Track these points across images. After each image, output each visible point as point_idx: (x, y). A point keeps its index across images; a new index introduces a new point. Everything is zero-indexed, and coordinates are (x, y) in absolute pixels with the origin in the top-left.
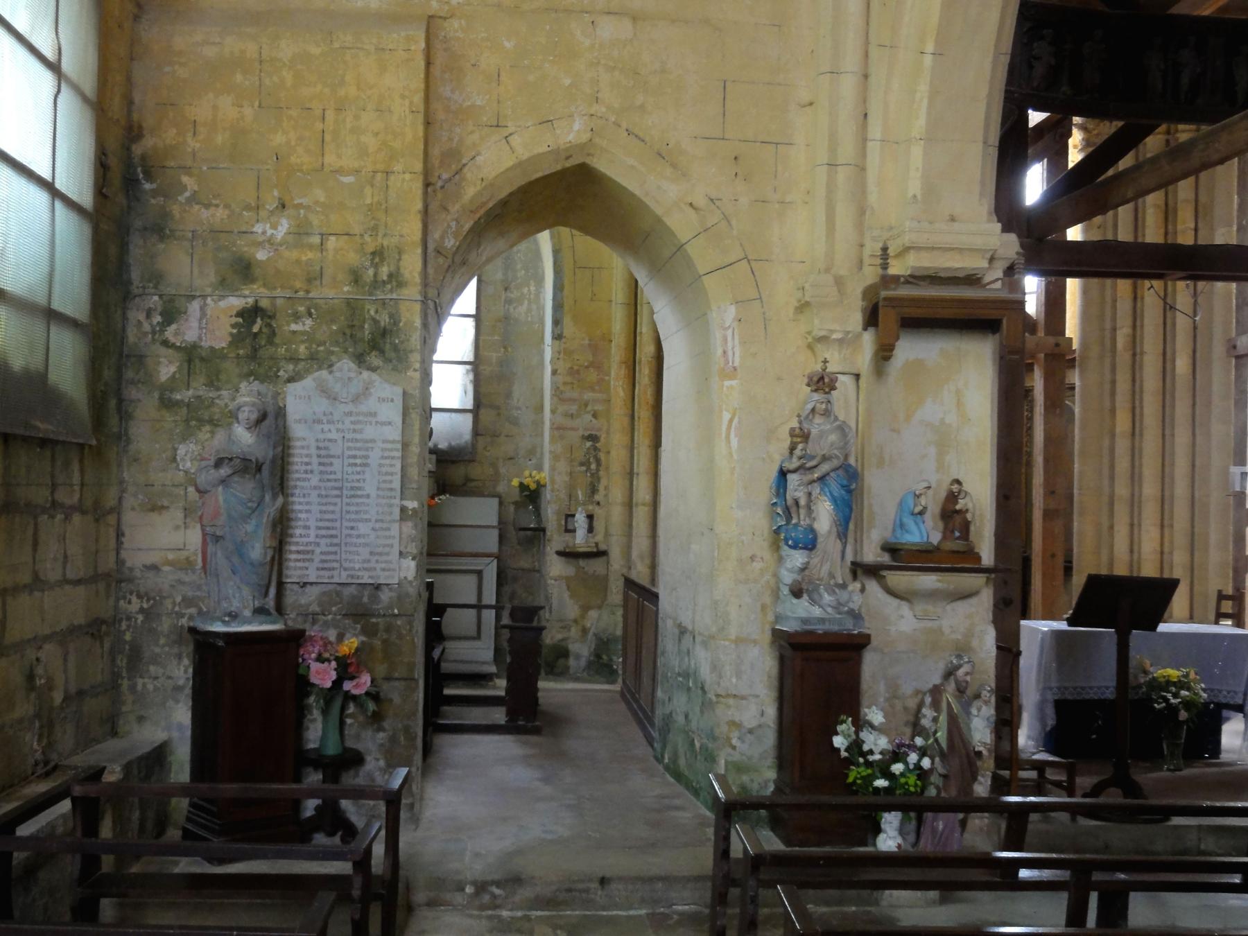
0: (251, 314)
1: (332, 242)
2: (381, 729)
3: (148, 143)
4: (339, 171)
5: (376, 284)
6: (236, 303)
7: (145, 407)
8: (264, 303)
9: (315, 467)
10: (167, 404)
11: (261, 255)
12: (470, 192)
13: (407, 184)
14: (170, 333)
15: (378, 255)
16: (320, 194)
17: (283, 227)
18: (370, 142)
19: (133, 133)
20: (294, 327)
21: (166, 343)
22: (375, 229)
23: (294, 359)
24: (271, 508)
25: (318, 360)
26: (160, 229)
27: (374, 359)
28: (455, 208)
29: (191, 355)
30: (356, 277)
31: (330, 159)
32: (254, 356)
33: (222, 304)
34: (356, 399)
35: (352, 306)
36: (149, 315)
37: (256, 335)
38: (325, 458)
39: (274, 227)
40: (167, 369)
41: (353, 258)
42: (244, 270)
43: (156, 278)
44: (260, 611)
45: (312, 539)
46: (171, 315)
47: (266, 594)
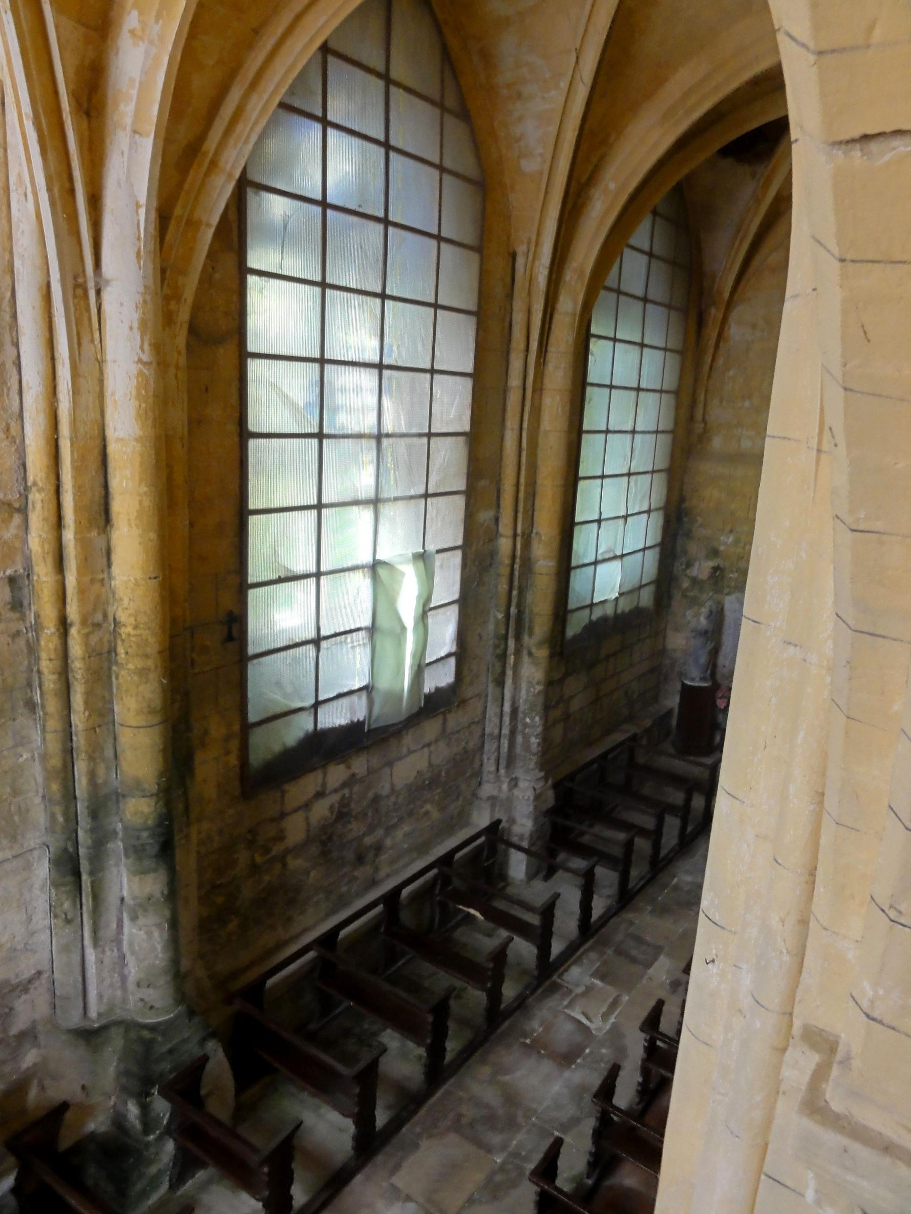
0: (716, 569)
3: (686, 505)
6: (711, 564)
7: (677, 596)
8: (721, 566)
10: (684, 596)
11: (722, 548)
14: (688, 571)
17: (731, 539)
19: (682, 500)
21: (686, 575)
23: (729, 586)
24: (710, 646)
26: (688, 535)
29: (695, 581)
32: (716, 583)
33: (706, 564)
36: (681, 565)
37: (717, 577)
39: (728, 538)
40: (686, 584)
42: (715, 553)
43: (685, 552)
44: (703, 679)
46: (689, 565)
47: (706, 671)
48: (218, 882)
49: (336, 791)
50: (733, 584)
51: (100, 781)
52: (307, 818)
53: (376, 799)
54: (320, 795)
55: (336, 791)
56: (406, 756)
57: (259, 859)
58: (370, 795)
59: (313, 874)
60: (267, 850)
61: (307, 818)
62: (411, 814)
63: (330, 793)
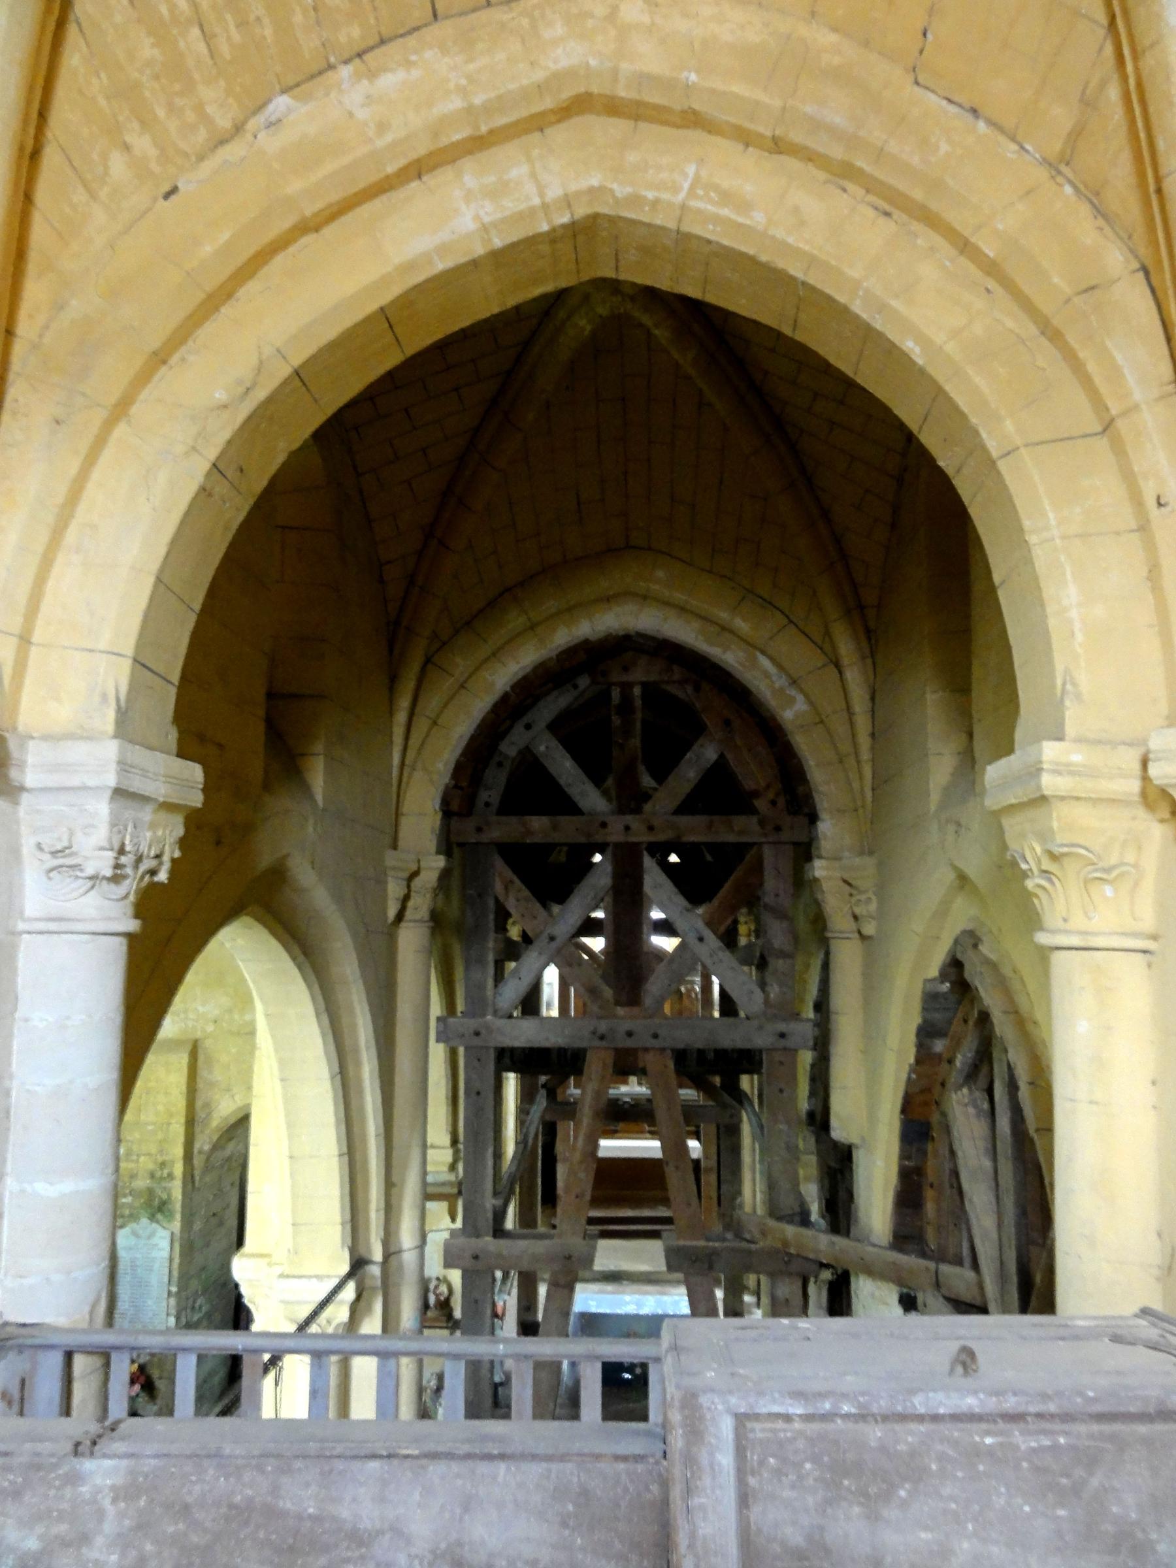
1: (142, 1159)
2: (155, 1404)
4: (147, 1124)
5: (162, 1179)
9: (129, 1271)
12: (215, 1123)
13: (178, 1129)
15: (163, 1165)
16: (137, 1135)
18: (160, 1108)
20: (124, 1200)
22: (162, 1151)
23: (122, 1216)
25: (134, 1217)
27: (159, 1216)
28: (207, 1132)
30: (152, 1176)
31: (143, 1117)
34: (149, 1237)
35: (150, 1192)
38: (134, 1267)
41: (151, 1166)
45: (127, 1307)
50: (127, 1212)
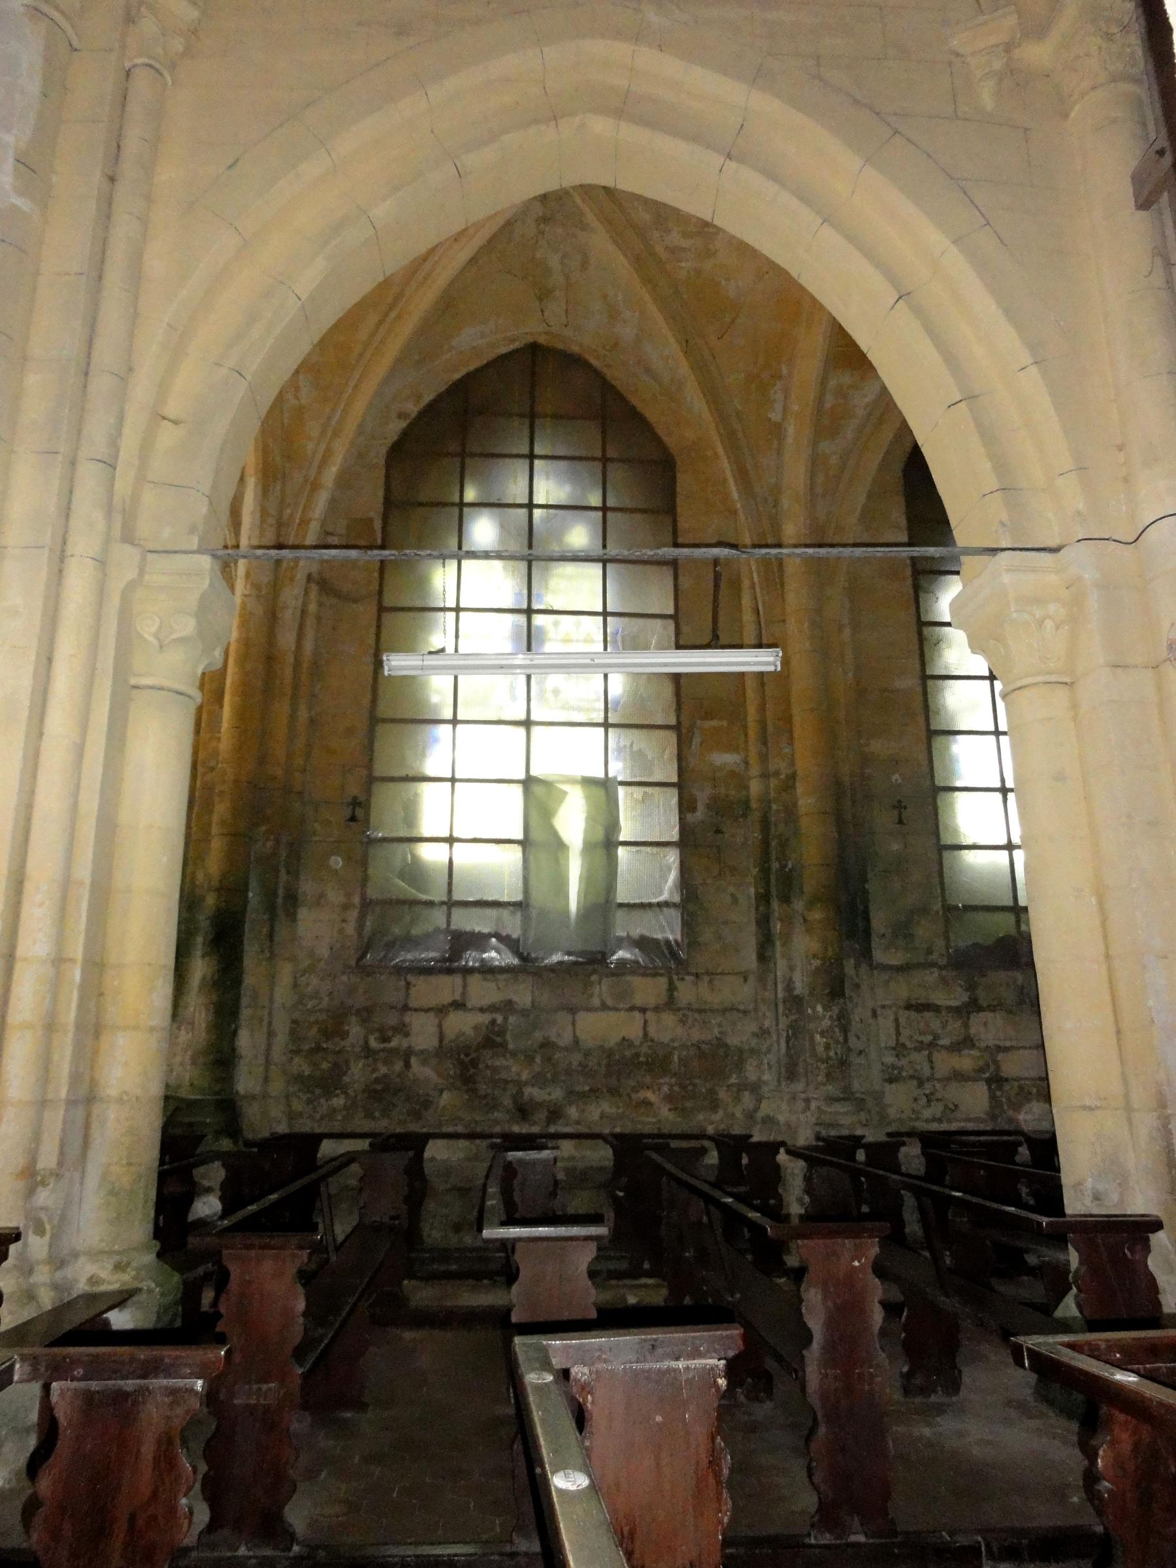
48: (325, 1046)
49: (482, 1010)
51: (197, 883)
52: (440, 1026)
53: (547, 1045)
54: (459, 1005)
55: (482, 1010)
56: (595, 1010)
57: (373, 1043)
58: (538, 1035)
59: (446, 1096)
60: (384, 1039)
61: (440, 1026)
62: (614, 1092)
63: (471, 1009)
